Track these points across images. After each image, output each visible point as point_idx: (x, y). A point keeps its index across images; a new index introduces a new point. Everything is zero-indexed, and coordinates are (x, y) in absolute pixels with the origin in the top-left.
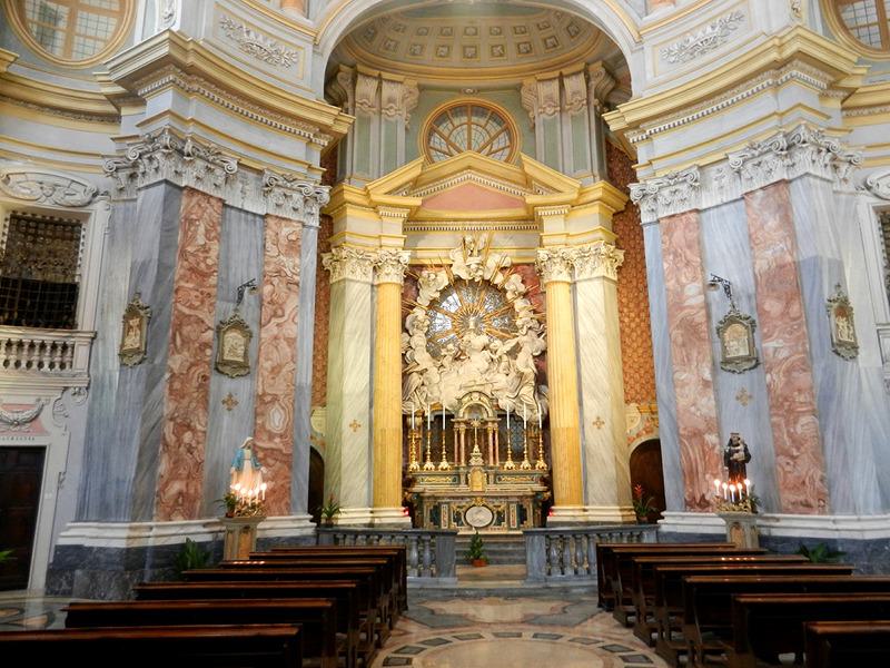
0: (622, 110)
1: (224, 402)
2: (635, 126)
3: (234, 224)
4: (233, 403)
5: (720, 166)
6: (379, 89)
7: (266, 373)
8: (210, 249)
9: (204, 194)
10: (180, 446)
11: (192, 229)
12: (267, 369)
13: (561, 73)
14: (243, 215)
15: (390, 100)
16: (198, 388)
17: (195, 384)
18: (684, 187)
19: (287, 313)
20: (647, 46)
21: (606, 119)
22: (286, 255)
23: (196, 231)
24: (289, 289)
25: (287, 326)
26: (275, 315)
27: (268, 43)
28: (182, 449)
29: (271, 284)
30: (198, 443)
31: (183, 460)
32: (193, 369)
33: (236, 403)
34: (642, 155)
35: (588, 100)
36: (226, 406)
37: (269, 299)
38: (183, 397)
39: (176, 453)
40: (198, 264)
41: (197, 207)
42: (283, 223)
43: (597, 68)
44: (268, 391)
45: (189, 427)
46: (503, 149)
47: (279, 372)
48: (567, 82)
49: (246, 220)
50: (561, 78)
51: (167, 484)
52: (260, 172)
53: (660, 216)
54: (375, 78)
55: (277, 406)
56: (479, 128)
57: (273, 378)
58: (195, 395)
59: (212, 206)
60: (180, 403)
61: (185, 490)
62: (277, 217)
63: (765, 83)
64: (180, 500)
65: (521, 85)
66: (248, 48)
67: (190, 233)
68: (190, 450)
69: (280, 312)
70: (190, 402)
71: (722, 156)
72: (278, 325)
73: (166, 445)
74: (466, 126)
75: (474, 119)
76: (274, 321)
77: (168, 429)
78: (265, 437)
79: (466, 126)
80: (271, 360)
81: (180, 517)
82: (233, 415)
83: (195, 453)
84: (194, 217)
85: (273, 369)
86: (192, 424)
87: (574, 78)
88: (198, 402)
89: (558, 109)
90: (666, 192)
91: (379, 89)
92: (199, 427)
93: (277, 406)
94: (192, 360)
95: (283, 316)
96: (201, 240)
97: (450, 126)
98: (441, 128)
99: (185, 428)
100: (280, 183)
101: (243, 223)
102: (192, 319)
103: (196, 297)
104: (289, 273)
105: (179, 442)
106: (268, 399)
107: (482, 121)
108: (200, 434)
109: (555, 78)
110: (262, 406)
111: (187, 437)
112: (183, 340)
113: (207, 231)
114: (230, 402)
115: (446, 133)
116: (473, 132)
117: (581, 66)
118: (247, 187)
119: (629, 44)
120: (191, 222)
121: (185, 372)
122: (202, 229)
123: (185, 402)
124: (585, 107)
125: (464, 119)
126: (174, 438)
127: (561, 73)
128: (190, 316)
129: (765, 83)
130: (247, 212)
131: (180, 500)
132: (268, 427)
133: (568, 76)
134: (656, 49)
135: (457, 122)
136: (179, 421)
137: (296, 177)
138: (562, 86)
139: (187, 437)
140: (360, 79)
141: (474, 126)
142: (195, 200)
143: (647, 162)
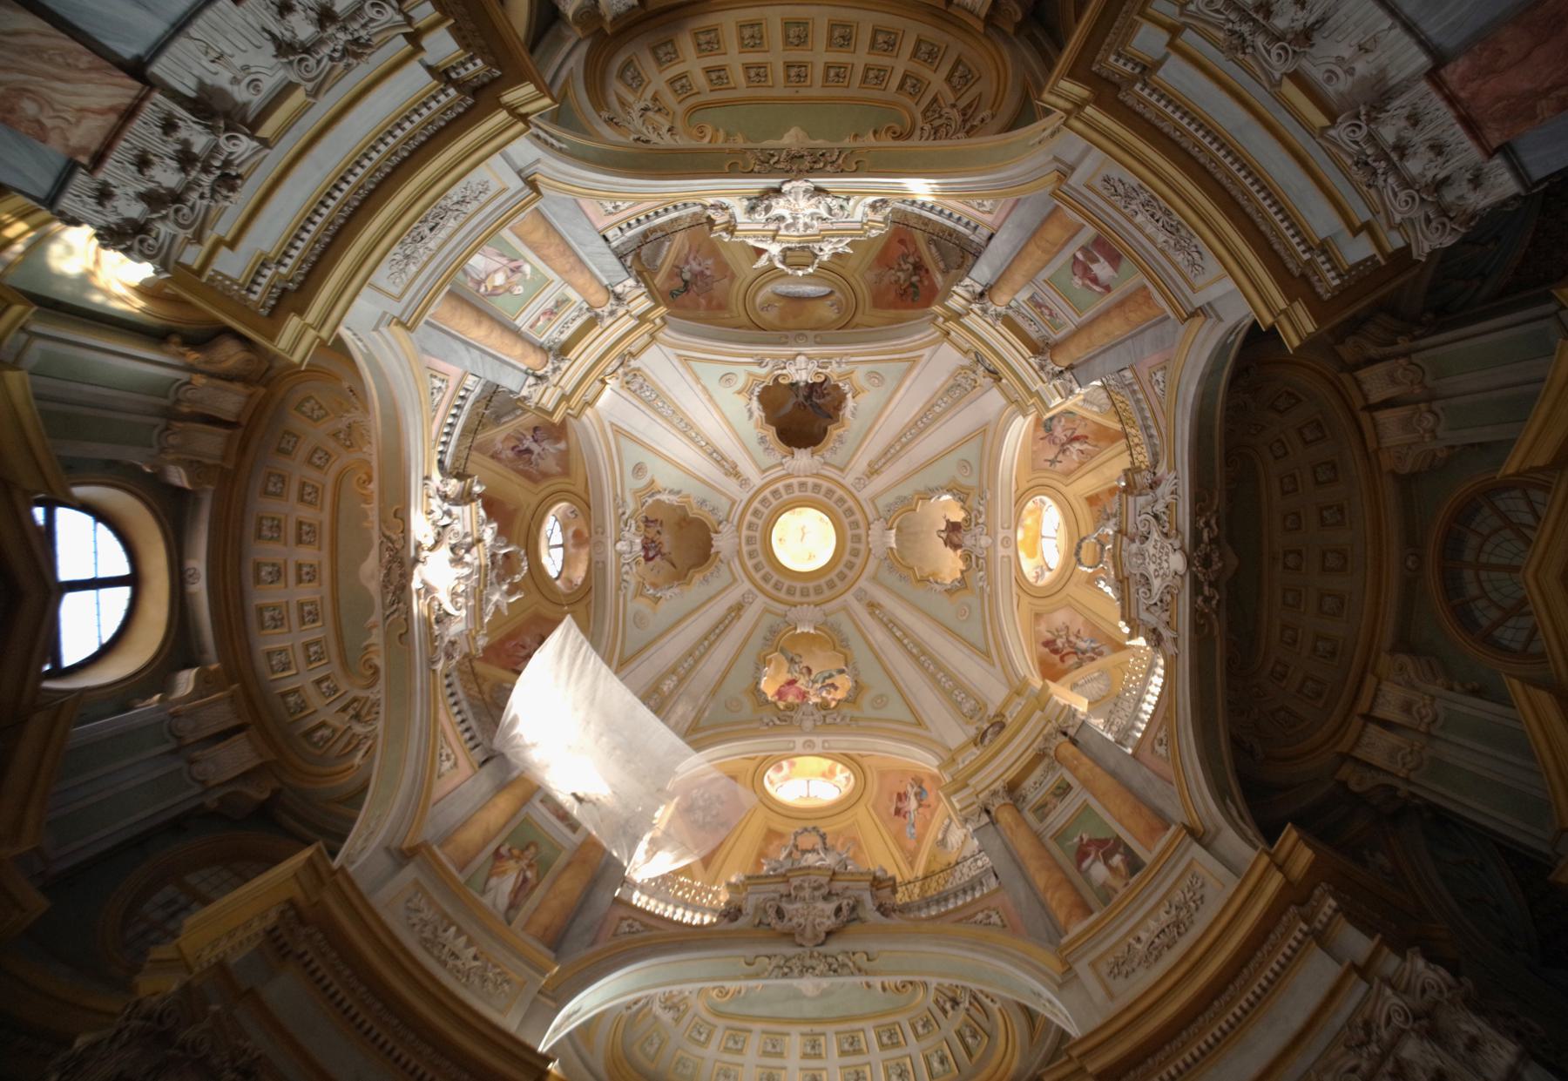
0: (1269, 320)
2: (1296, 284)
5: (1317, 74)
6: (1387, 725)
13: (1364, 409)
15: (1407, 708)
18: (1388, 134)
20: (1198, 300)
21: (1296, 343)
27: (1164, 917)
34: (1358, 250)
35: (1396, 356)
43: (1347, 351)
46: (1530, 503)
48: (1375, 398)
50: (1371, 408)
53: (1474, 154)
54: (1364, 726)
56: (1488, 547)
63: (1145, 93)
65: (1394, 474)
66: (1154, 952)
71: (1290, 90)
74: (1483, 575)
75: (1469, 556)
79: (1483, 575)
87: (1366, 387)
89: (1423, 406)
90: (1414, 166)
91: (1387, 725)
97: (1481, 603)
98: (1484, 622)
107: (1473, 541)
109: (1373, 418)
115: (1495, 614)
116: (1493, 560)
117: (1345, 377)
119: (1212, 328)
124: (1415, 358)
125: (1468, 574)
127: (1364, 409)
129: (1145, 93)
133: (1365, 397)
134: (1199, 282)
135: (1473, 590)
138: (1388, 404)
140: (1359, 753)
141: (1483, 559)
143: (1364, 237)
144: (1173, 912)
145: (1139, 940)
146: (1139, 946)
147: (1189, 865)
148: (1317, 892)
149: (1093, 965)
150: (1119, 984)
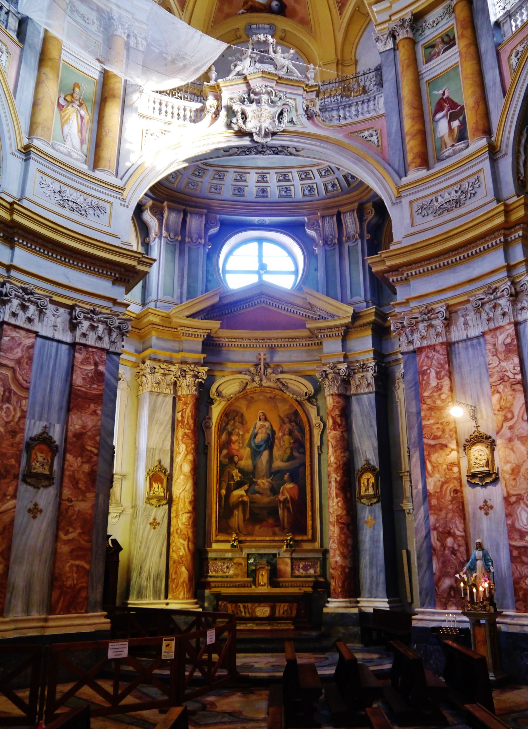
1: (481, 508)
3: (463, 352)
4: (489, 507)
7: (507, 476)
8: (442, 386)
9: (428, 347)
10: (444, 550)
11: (425, 378)
12: (507, 472)
14: (469, 343)
16: (452, 501)
17: (448, 498)
19: (516, 414)
22: (506, 359)
23: (428, 378)
24: (514, 390)
25: (518, 426)
26: (506, 419)
28: (447, 552)
29: (498, 392)
30: (459, 546)
31: (449, 560)
32: (445, 487)
33: (492, 507)
36: (483, 512)
37: (498, 407)
38: (441, 510)
39: (443, 555)
40: (435, 402)
41: (426, 359)
42: (498, 332)
44: (512, 492)
45: (450, 534)
47: (519, 472)
49: (472, 345)
51: (439, 579)
52: (468, 301)
55: (522, 505)
57: (515, 479)
58: (450, 507)
59: (438, 352)
60: (438, 515)
61: (455, 585)
62: (490, 330)
64: (452, 593)
67: (424, 382)
68: (454, 552)
69: (509, 416)
70: (447, 514)
72: (511, 428)
73: (434, 550)
76: (506, 425)
77: (434, 535)
78: (517, 536)
80: (510, 462)
81: (454, 608)
82: (490, 518)
83: (459, 555)
84: (425, 368)
85: (513, 470)
86: (452, 531)
88: (454, 512)
92: (458, 533)
93: (522, 505)
94: (443, 479)
95: (513, 417)
96: (433, 383)
99: (446, 535)
100: (486, 300)
101: (470, 350)
102: (437, 446)
103: (438, 428)
104: (511, 376)
105: (444, 545)
106: (513, 499)
108: (460, 539)
110: (509, 508)
111: (450, 541)
112: (433, 467)
113: (437, 373)
114: (486, 507)
118: (468, 318)
120: (424, 373)
121: (439, 490)
122: (433, 374)
123: (443, 514)
126: (439, 544)
128: (436, 445)
130: (471, 339)
131: (452, 593)
132: (517, 526)
136: (440, 530)
137: (493, 287)
139: (450, 541)
142: (423, 355)
144: (459, 193)
145: (437, 200)
146: (435, 203)
147: (479, 171)
148: (517, 227)
149: (411, 202)
150: (418, 219)
